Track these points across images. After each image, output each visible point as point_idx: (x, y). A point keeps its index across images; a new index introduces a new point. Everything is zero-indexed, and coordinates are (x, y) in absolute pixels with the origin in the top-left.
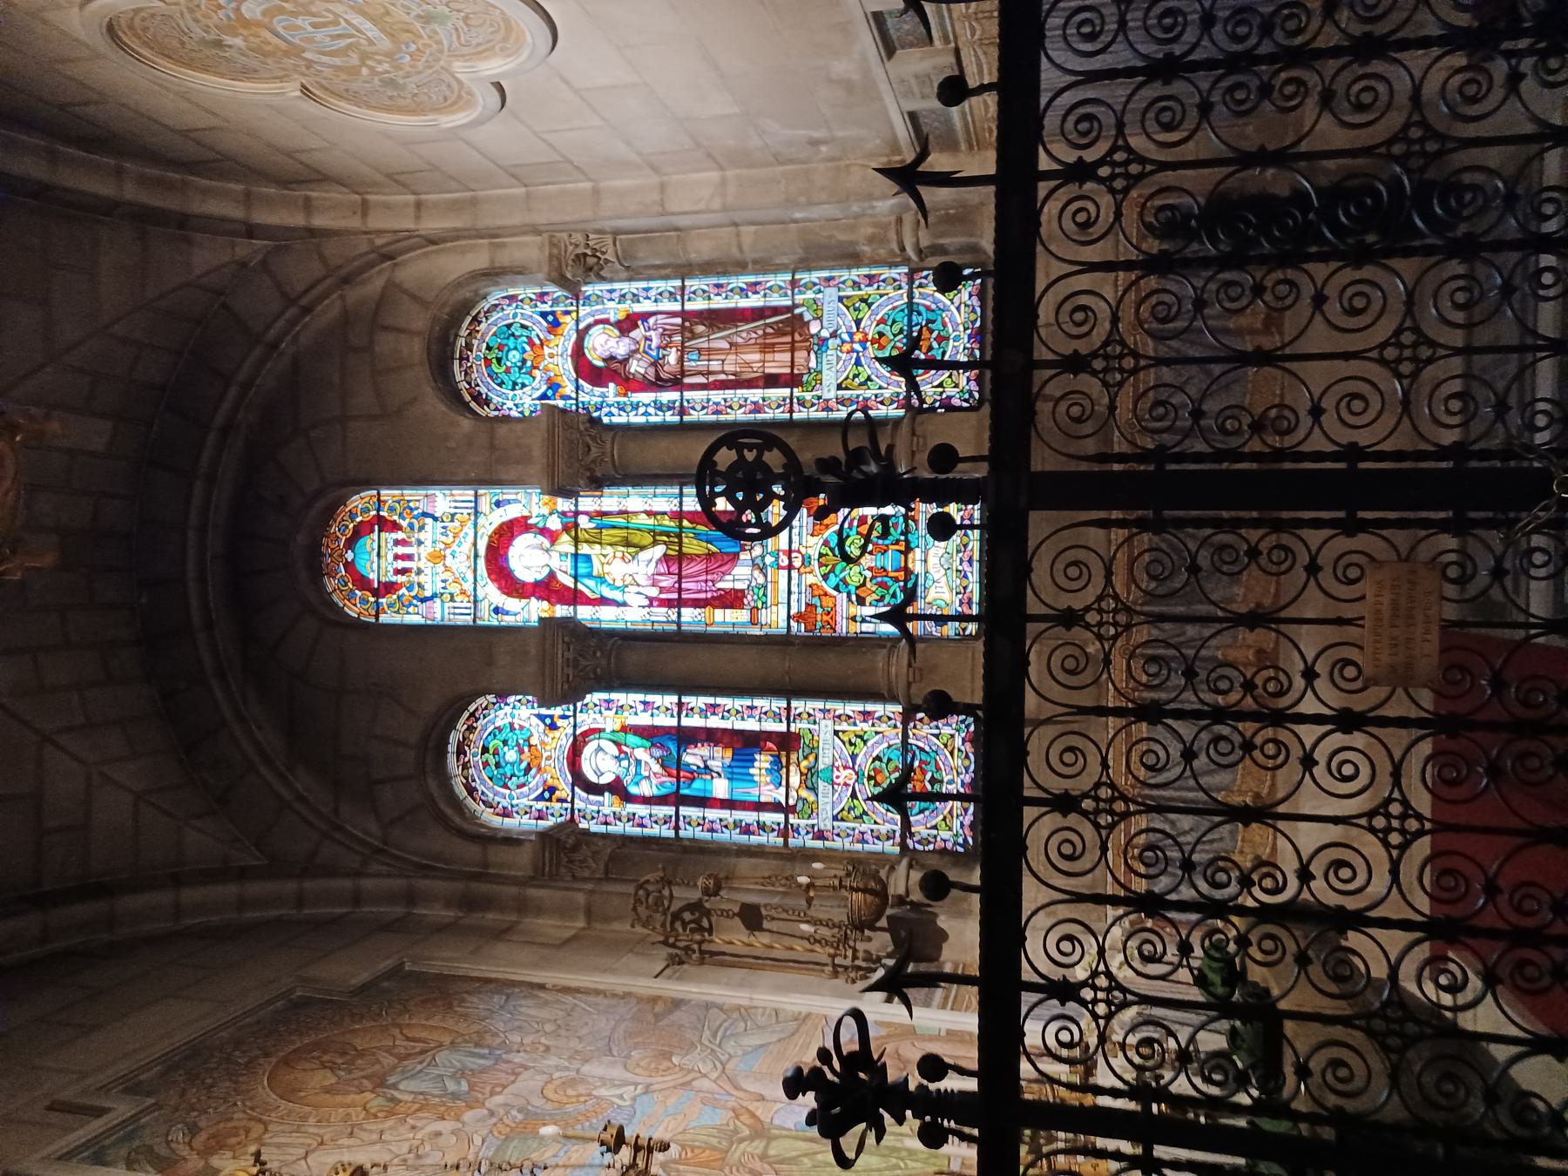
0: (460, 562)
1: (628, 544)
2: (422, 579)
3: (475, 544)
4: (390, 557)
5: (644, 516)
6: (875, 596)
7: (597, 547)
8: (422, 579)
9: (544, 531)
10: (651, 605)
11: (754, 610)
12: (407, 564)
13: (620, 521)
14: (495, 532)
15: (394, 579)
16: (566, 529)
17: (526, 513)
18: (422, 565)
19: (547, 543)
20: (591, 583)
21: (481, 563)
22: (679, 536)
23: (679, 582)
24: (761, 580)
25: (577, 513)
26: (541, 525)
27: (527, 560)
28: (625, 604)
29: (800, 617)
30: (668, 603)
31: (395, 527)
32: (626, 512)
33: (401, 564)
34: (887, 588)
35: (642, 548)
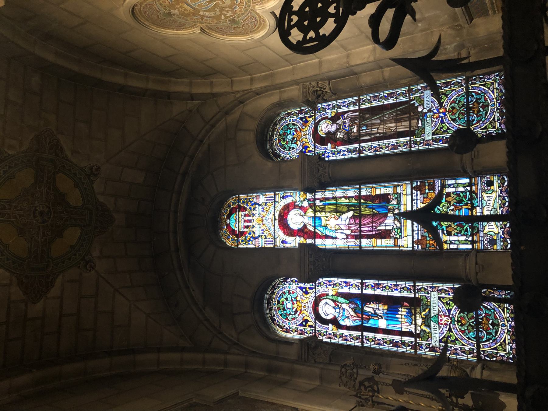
0: (269, 223)
1: (336, 211)
3: (274, 215)
5: (343, 199)
6: (456, 231)
7: (324, 213)
9: (301, 208)
10: (347, 238)
11: (395, 239)
12: (249, 224)
13: (333, 202)
14: (282, 209)
16: (310, 206)
19: (303, 213)
20: (321, 229)
21: (277, 222)
22: (359, 207)
23: (360, 227)
24: (398, 225)
25: (315, 199)
26: (300, 205)
27: (295, 220)
28: (336, 238)
29: (418, 242)
30: (355, 237)
31: (245, 209)
32: (336, 198)
33: (246, 224)
34: (463, 227)
35: (343, 213)
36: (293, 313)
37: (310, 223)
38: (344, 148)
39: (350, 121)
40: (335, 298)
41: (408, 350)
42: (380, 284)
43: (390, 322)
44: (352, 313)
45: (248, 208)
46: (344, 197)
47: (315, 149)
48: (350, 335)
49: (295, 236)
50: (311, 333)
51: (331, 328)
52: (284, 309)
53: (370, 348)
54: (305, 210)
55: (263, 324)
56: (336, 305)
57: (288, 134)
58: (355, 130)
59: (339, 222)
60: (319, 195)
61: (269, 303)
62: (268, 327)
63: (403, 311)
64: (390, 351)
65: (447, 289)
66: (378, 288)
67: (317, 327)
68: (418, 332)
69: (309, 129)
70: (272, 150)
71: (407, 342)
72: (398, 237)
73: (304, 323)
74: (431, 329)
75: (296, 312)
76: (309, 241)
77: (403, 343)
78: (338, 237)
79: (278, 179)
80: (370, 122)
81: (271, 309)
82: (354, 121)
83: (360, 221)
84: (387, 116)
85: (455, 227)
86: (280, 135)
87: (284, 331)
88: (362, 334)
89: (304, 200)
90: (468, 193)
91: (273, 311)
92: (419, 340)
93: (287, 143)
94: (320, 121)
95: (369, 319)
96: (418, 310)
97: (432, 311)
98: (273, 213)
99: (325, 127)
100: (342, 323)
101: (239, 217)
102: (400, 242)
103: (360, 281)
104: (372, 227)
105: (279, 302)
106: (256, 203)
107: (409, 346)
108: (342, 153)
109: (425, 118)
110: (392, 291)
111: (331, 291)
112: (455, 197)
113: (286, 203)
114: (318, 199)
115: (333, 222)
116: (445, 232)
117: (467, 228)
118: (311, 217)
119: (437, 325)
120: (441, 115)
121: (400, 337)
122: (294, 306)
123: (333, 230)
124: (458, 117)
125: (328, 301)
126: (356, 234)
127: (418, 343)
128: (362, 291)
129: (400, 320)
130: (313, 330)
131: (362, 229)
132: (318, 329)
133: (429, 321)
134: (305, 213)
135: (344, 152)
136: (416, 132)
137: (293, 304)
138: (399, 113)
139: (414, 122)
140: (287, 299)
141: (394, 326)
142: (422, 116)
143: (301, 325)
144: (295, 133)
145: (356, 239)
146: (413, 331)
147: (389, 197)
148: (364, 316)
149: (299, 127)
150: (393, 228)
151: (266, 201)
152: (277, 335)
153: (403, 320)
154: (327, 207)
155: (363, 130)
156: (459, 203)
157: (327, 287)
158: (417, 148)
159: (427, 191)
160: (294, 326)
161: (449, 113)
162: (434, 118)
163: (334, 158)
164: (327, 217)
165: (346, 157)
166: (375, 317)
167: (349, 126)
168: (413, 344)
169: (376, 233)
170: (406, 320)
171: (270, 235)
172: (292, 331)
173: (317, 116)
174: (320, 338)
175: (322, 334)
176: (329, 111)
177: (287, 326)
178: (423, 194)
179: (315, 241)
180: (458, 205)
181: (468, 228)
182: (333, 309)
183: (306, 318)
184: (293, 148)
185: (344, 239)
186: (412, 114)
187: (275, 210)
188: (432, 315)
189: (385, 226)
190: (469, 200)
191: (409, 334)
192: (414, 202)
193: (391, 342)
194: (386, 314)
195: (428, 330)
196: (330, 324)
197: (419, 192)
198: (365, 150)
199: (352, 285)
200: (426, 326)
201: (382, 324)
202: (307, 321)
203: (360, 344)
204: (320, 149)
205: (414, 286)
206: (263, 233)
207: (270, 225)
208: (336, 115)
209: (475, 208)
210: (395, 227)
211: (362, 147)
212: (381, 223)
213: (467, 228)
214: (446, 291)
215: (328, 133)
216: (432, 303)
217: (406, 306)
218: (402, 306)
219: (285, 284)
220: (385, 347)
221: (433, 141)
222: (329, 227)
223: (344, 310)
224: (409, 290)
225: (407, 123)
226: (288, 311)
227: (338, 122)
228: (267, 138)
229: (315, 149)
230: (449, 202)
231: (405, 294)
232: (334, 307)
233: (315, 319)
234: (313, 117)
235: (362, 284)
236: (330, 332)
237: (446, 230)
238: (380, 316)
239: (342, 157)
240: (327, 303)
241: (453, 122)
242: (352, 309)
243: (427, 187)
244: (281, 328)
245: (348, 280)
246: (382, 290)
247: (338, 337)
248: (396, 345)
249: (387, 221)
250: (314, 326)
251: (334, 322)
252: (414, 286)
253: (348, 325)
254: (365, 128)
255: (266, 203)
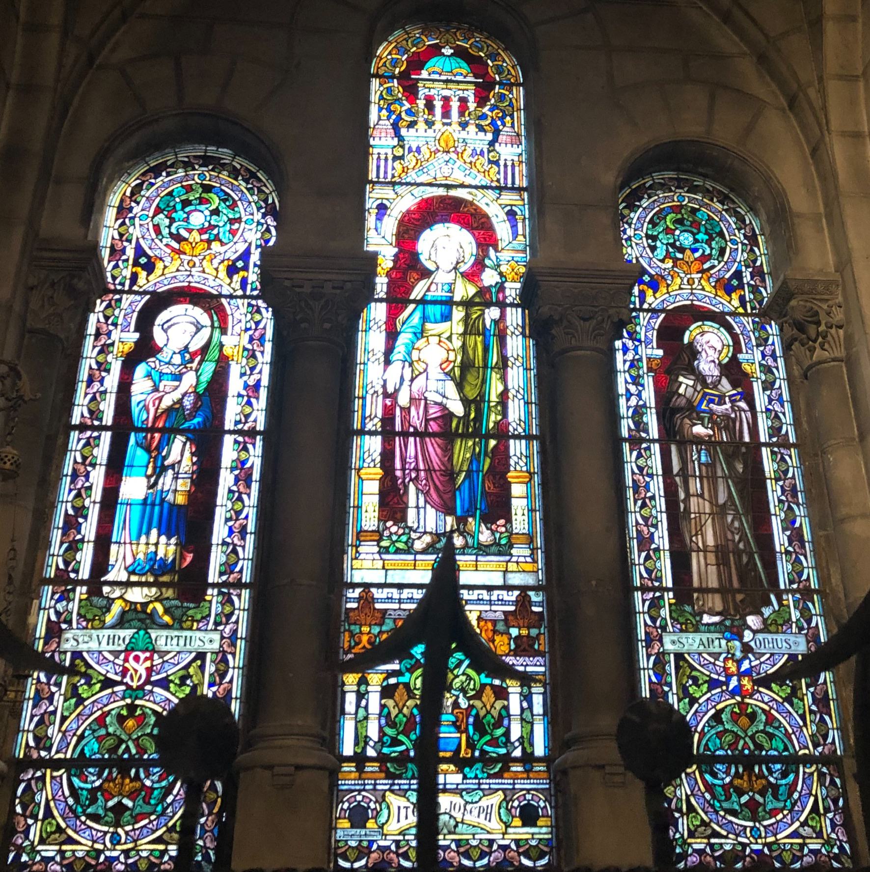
1: (466, 366)
3: (462, 186)
5: (501, 388)
6: (394, 712)
7: (460, 329)
9: (479, 265)
10: (386, 395)
11: (378, 535)
13: (494, 358)
14: (477, 209)
16: (483, 291)
19: (464, 268)
21: (441, 192)
22: (476, 433)
23: (416, 434)
24: (418, 545)
25: (502, 305)
26: (487, 262)
27: (445, 246)
28: (388, 362)
30: (388, 418)
35: (460, 387)
36: (174, 231)
37: (433, 287)
38: (649, 395)
39: (726, 416)
40: (214, 354)
41: (54, 562)
42: (249, 486)
43: (137, 511)
44: (167, 402)
47: (648, 311)
48: (105, 392)
49: (398, 244)
50: (114, 278)
51: (126, 338)
52: (186, 203)
53: (65, 449)
54: (473, 275)
55: (146, 142)
56: (193, 355)
58: (698, 429)
59: (435, 372)
60: (514, 317)
61: (206, 161)
62: (137, 155)
63: (167, 549)
64: (53, 506)
65: (227, 679)
66: (237, 480)
67: (132, 297)
68: (106, 589)
69: (707, 296)
70: (651, 187)
71: (78, 557)
72: (385, 543)
73: (143, 260)
74: (113, 627)
75: (178, 238)
76: (381, 284)
77: (74, 547)
78: (390, 368)
79: (567, 199)
80: (719, 473)
81: (188, 165)
82: (726, 428)
83: (433, 435)
84: (736, 524)
85: (405, 710)
86: (694, 211)
87: (122, 201)
88: (106, 428)
89: (501, 274)
90: (503, 751)
91: (181, 173)
92: (81, 592)
93: (668, 231)
94: (729, 328)
95: (148, 450)
96: (169, 593)
97: (165, 633)
98: (468, 181)
99: (710, 343)
100: (141, 370)
102: (369, 549)
103: (260, 427)
104: (417, 469)
105: (207, 189)
107: (67, 563)
108: (633, 389)
109: (728, 635)
110: (227, 520)
111: (233, 342)
112: (495, 713)
113: (494, 220)
114: (503, 316)
116: (393, 681)
117: (401, 743)
118: (451, 291)
119: (123, 647)
120: (734, 682)
121: (92, 538)
122: (195, 234)
123: (409, 354)
124: (726, 731)
125: (205, 334)
127: (74, 590)
128: (231, 432)
129: (143, 539)
130: (123, 284)
131: (411, 439)
132: (127, 300)
133: (135, 623)
134: (463, 275)
135: (636, 395)
136: (688, 608)
137: (202, 231)
138: (745, 559)
139: (716, 602)
140: (216, 212)
141: (127, 520)
142: (732, 626)
143: (140, 251)
145: (382, 420)
146: (110, 577)
147: (501, 522)
148: (157, 435)
149: (713, 267)
150: (411, 528)
152: (111, 181)
153: (142, 548)
154: (479, 339)
155: (699, 452)
156: (474, 725)
157: (247, 330)
158: (639, 607)
159: (514, 632)
160: (136, 232)
161: (738, 703)
162: (726, 659)
163: (620, 366)
164: (449, 338)
165: (622, 401)
166: (155, 468)
167: (711, 412)
168: (72, 575)
169: (396, 478)
170: (141, 556)
172: (123, 224)
173: (744, 320)
174: (100, 306)
175: (109, 312)
176: (758, 356)
177: (137, 209)
178: (506, 621)
179: (381, 300)
180: (471, 720)
181: (403, 748)
182: (182, 346)
183: (159, 265)
184: (653, 249)
185: (384, 386)
186: (739, 597)
187: (476, 187)
188: (154, 634)
189: (417, 507)
190: (483, 752)
191: (101, 564)
192: (484, 595)
193: (81, 511)
194: (163, 500)
195: (109, 619)
196: (137, 335)
197: (512, 608)
198: (639, 456)
199: (249, 403)
200: (123, 613)
201: (133, 487)
202: (149, 268)
203: (76, 420)
204: (647, 327)
205: (239, 585)
208: (746, 375)
209: (460, 770)
210: (414, 535)
211: (648, 448)
212: (427, 494)
213: (401, 743)
214: (223, 676)
215: (693, 352)
216: (188, 633)
217: (182, 558)
218: (182, 547)
219: (259, 209)
220: (66, 494)
221: (658, 654)
222: (421, 343)
223: (178, 377)
224: (228, 568)
225: (713, 582)
226: (181, 215)
227: (724, 381)
228: (685, 172)
229: (648, 311)
230: (478, 695)
231: (217, 558)
232: (186, 348)
233: (153, 293)
234: (741, 310)
235: (252, 433)
236: (116, 335)
237: (397, 684)
238: (156, 483)
239: (621, 390)
240: (198, 330)
241: (713, 717)
242: (180, 401)
243: (524, 632)
244: (133, 194)
245: (263, 393)
246: (230, 491)
247: (101, 358)
248: (72, 524)
249: (431, 512)
250: (135, 288)
251: (145, 349)
252: (239, 585)
253: (134, 389)
254: (703, 459)
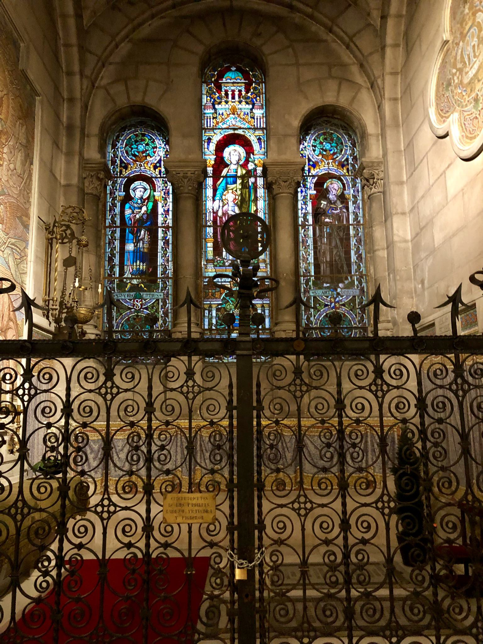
0: (231, 121)
2: (223, 103)
3: (240, 128)
4: (233, 88)
5: (255, 208)
7: (240, 187)
8: (223, 103)
10: (214, 212)
11: (212, 261)
12: (230, 96)
13: (253, 197)
15: (223, 90)
17: (255, 152)
18: (230, 103)
19: (241, 163)
20: (223, 184)
21: (232, 132)
24: (227, 264)
25: (256, 177)
26: (250, 160)
27: (234, 153)
28: (214, 200)
30: (215, 221)
33: (230, 93)
37: (230, 171)
45: (249, 95)
46: (257, 209)
57: (330, 144)
59: (231, 204)
60: (260, 181)
72: (216, 264)
76: (210, 170)
89: (255, 165)
98: (242, 126)
101: (238, 83)
106: (253, 105)
115: (230, 197)
118: (237, 172)
123: (222, 197)
126: (218, 222)
144: (332, 152)
151: (256, 118)
164: (236, 191)
171: (218, 123)
179: (210, 177)
184: (314, 151)
185: (213, 209)
187: (246, 129)
206: (219, 114)
207: (228, 123)
255: (254, 118)
